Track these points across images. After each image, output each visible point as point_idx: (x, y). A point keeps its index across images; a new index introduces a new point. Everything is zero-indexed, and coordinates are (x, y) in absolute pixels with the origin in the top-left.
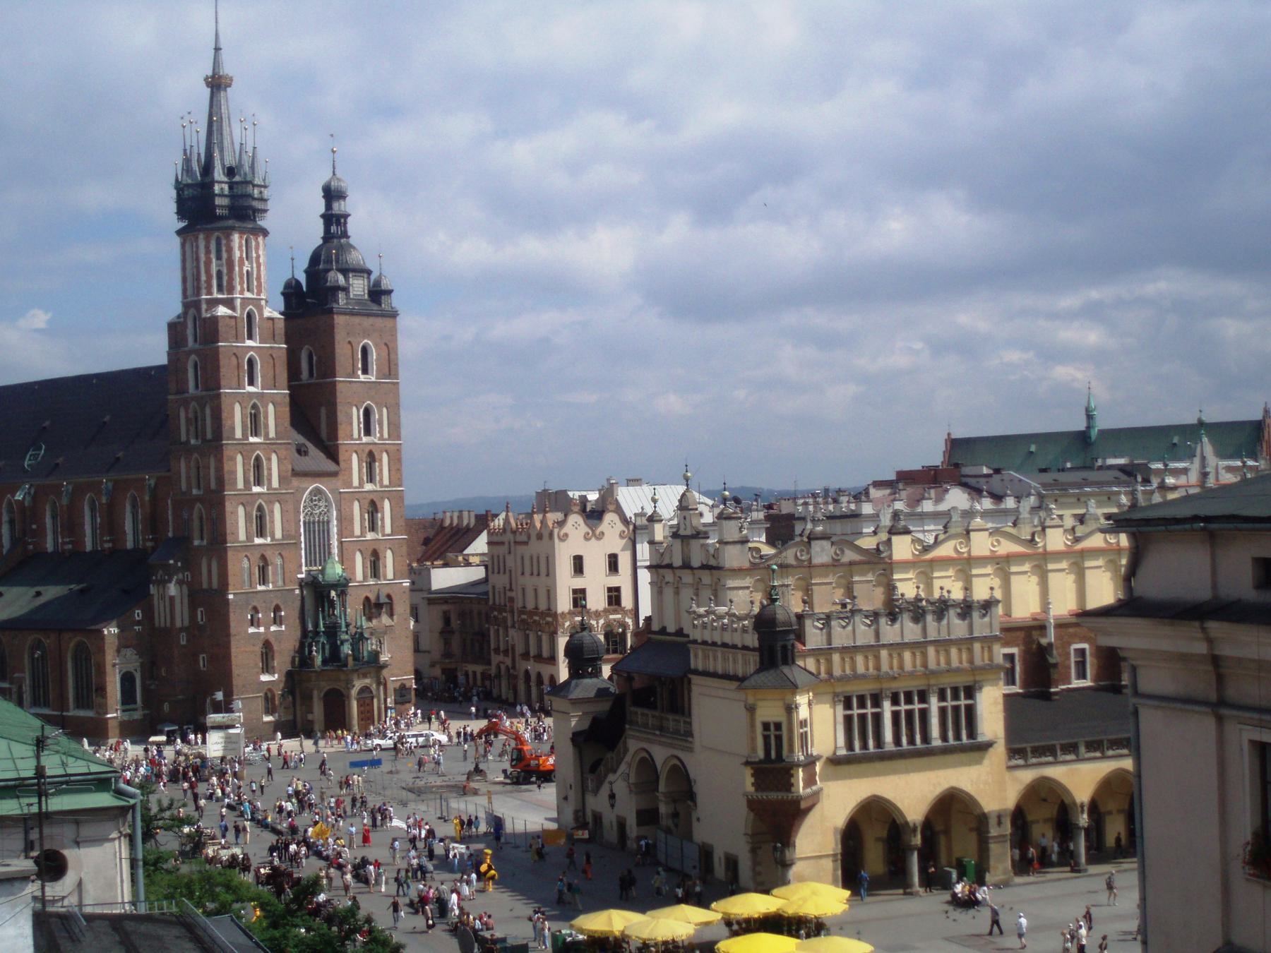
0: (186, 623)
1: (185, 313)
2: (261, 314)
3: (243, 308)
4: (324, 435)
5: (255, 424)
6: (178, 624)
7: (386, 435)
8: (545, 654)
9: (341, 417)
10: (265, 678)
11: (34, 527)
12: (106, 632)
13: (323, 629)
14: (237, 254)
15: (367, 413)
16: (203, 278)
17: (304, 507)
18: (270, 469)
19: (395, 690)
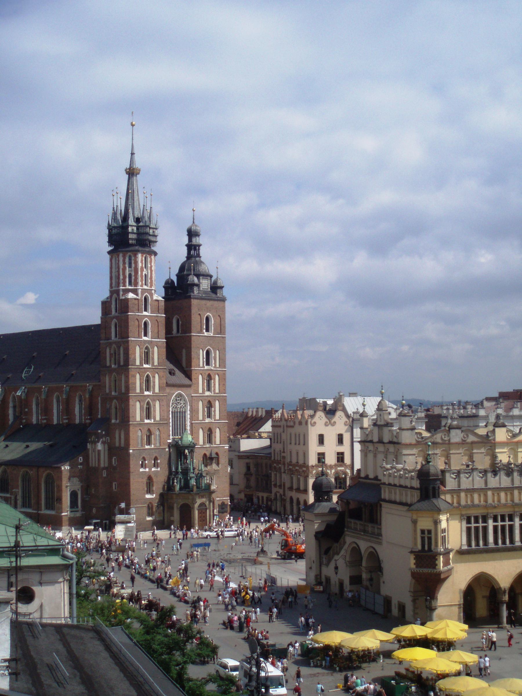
0: (106, 465)
1: (111, 297)
2: (152, 298)
3: (142, 294)
4: (184, 364)
5: (147, 357)
6: (102, 465)
7: (218, 366)
8: (302, 488)
9: (193, 354)
10: (148, 496)
11: (26, 410)
12: (63, 469)
13: (181, 471)
14: (140, 265)
15: (208, 353)
16: (121, 277)
18: (154, 382)
19: (219, 505)
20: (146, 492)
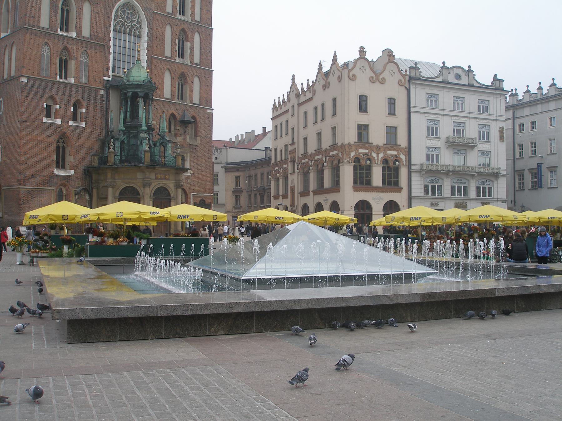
10: (57, 172)
17: (116, 16)
20: (55, 164)
